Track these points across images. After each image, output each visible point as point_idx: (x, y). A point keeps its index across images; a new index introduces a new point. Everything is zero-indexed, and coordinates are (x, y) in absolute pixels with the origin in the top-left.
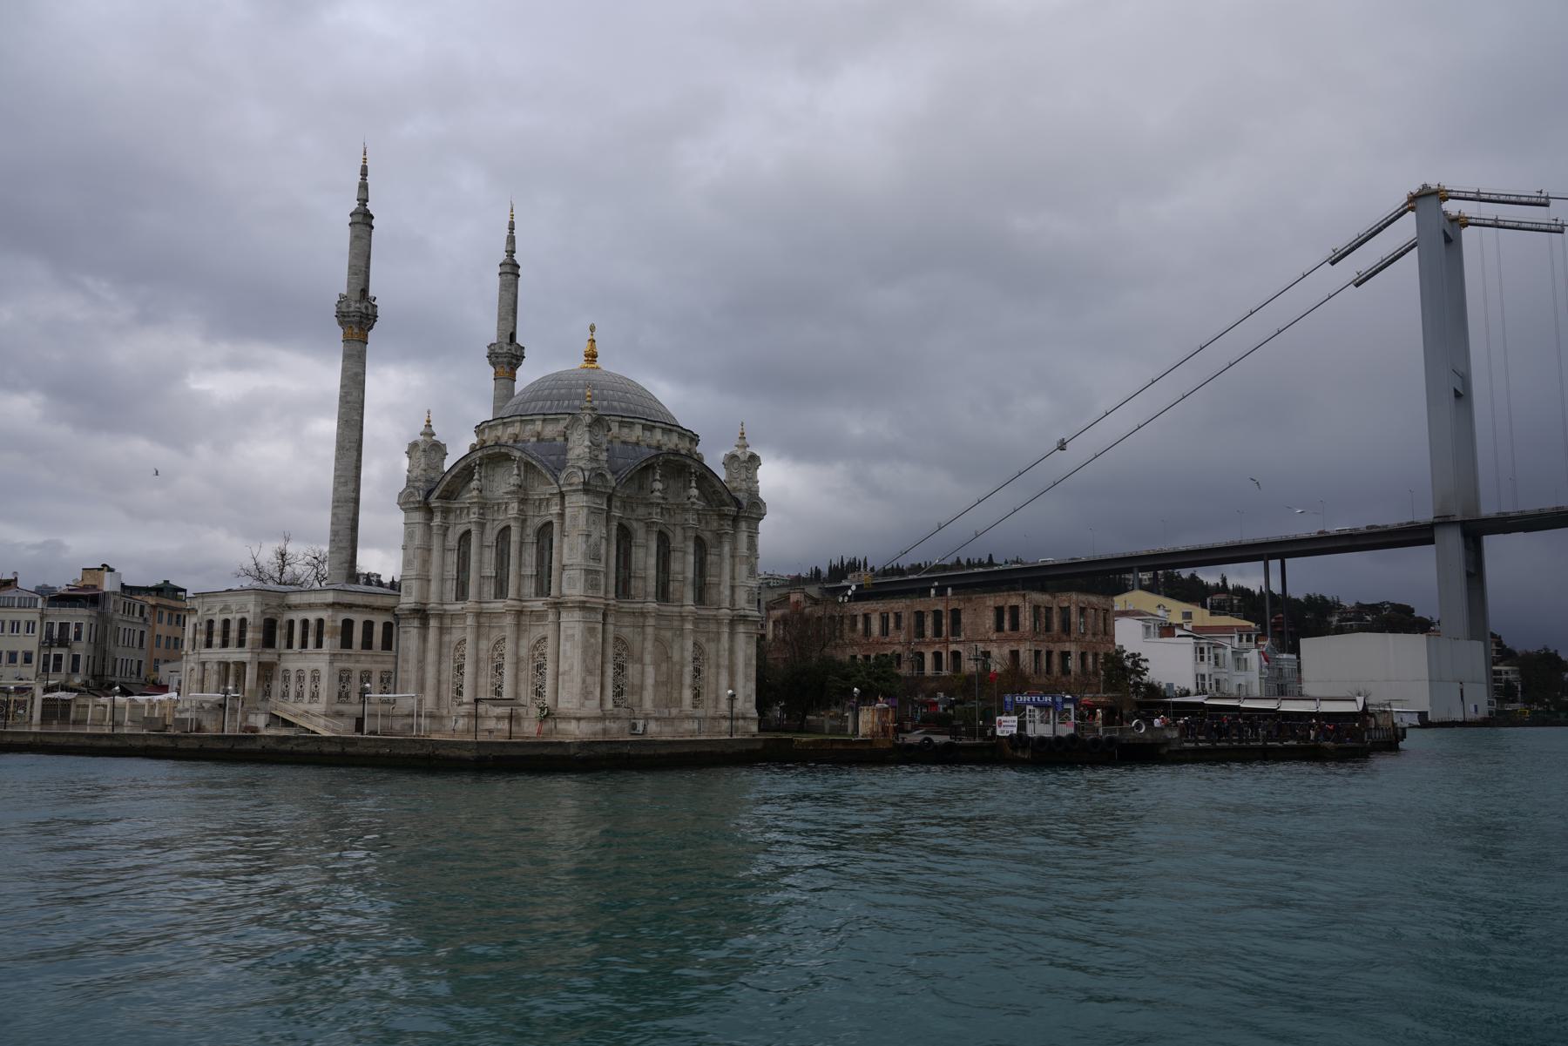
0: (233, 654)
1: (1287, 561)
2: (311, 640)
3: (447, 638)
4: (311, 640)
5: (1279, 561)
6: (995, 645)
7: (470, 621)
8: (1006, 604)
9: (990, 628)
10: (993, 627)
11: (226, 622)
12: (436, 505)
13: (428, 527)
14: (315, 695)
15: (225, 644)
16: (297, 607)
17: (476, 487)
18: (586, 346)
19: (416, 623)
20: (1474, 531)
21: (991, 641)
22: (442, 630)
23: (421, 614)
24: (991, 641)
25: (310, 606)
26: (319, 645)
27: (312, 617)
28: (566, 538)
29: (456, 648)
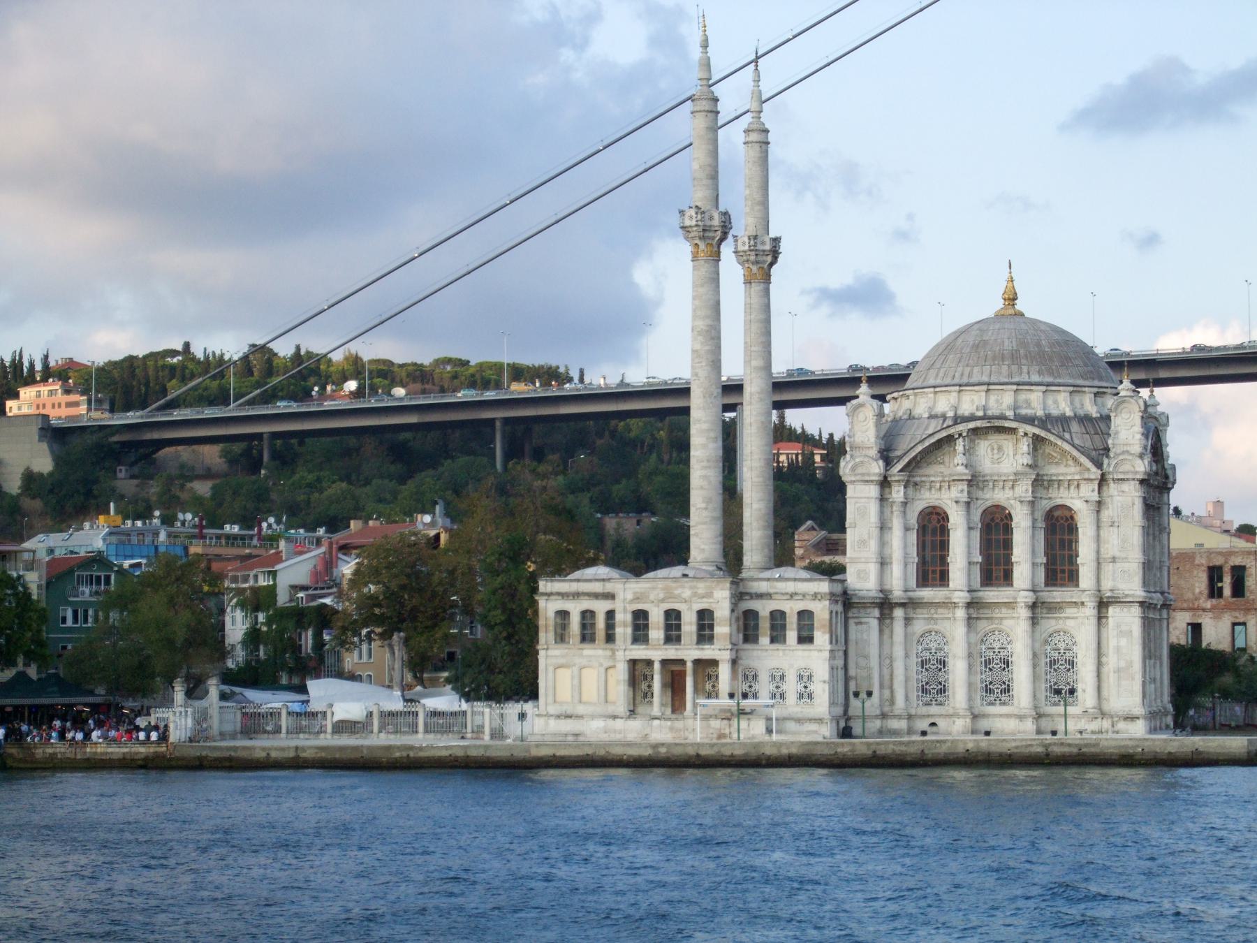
0: (689, 651)
2: (792, 635)
3: (910, 629)
4: (792, 635)
6: (1210, 615)
7: (961, 613)
8: (1226, 562)
9: (1201, 593)
10: (1206, 592)
11: (673, 619)
12: (897, 478)
13: (882, 499)
14: (805, 695)
16: (768, 596)
17: (960, 462)
18: (1002, 286)
19: (876, 613)
21: (1204, 610)
22: (908, 620)
23: (885, 605)
24: (1204, 610)
26: (806, 638)
27: (791, 608)
28: (1115, 529)
29: (919, 641)
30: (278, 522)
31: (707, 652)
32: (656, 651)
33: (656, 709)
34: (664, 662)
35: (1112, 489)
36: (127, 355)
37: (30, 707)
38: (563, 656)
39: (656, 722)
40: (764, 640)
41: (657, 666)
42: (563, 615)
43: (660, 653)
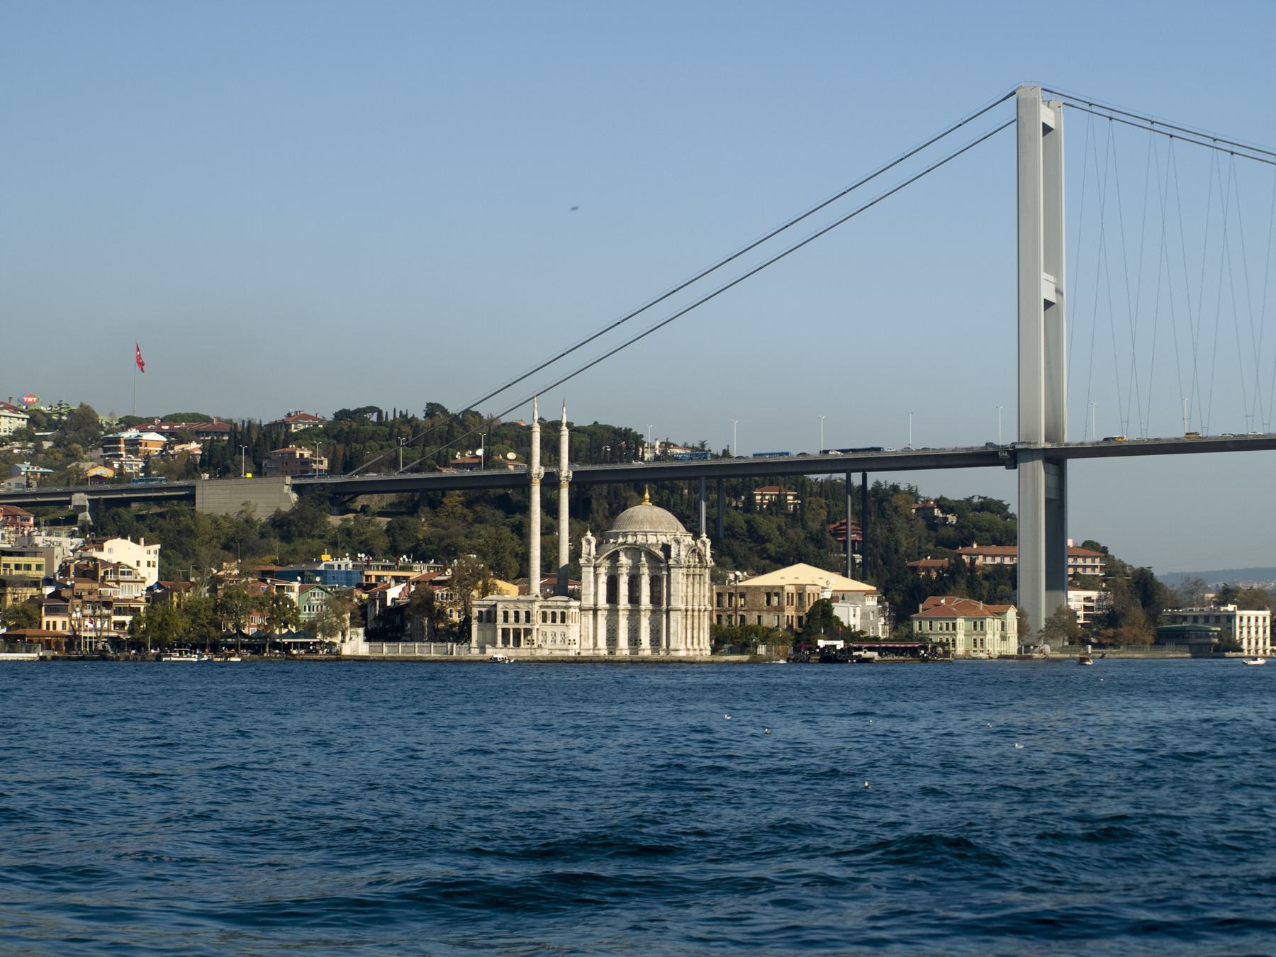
0: (522, 625)
1: (869, 474)
2: (558, 620)
4: (558, 620)
5: (860, 474)
11: (517, 614)
15: (517, 620)
19: (591, 612)
20: (1056, 459)
25: (558, 607)
26: (563, 621)
30: (408, 557)
31: (528, 626)
32: (511, 625)
33: (511, 646)
34: (514, 629)
35: (672, 570)
36: (341, 409)
37: (295, 643)
40: (549, 622)
41: (511, 631)
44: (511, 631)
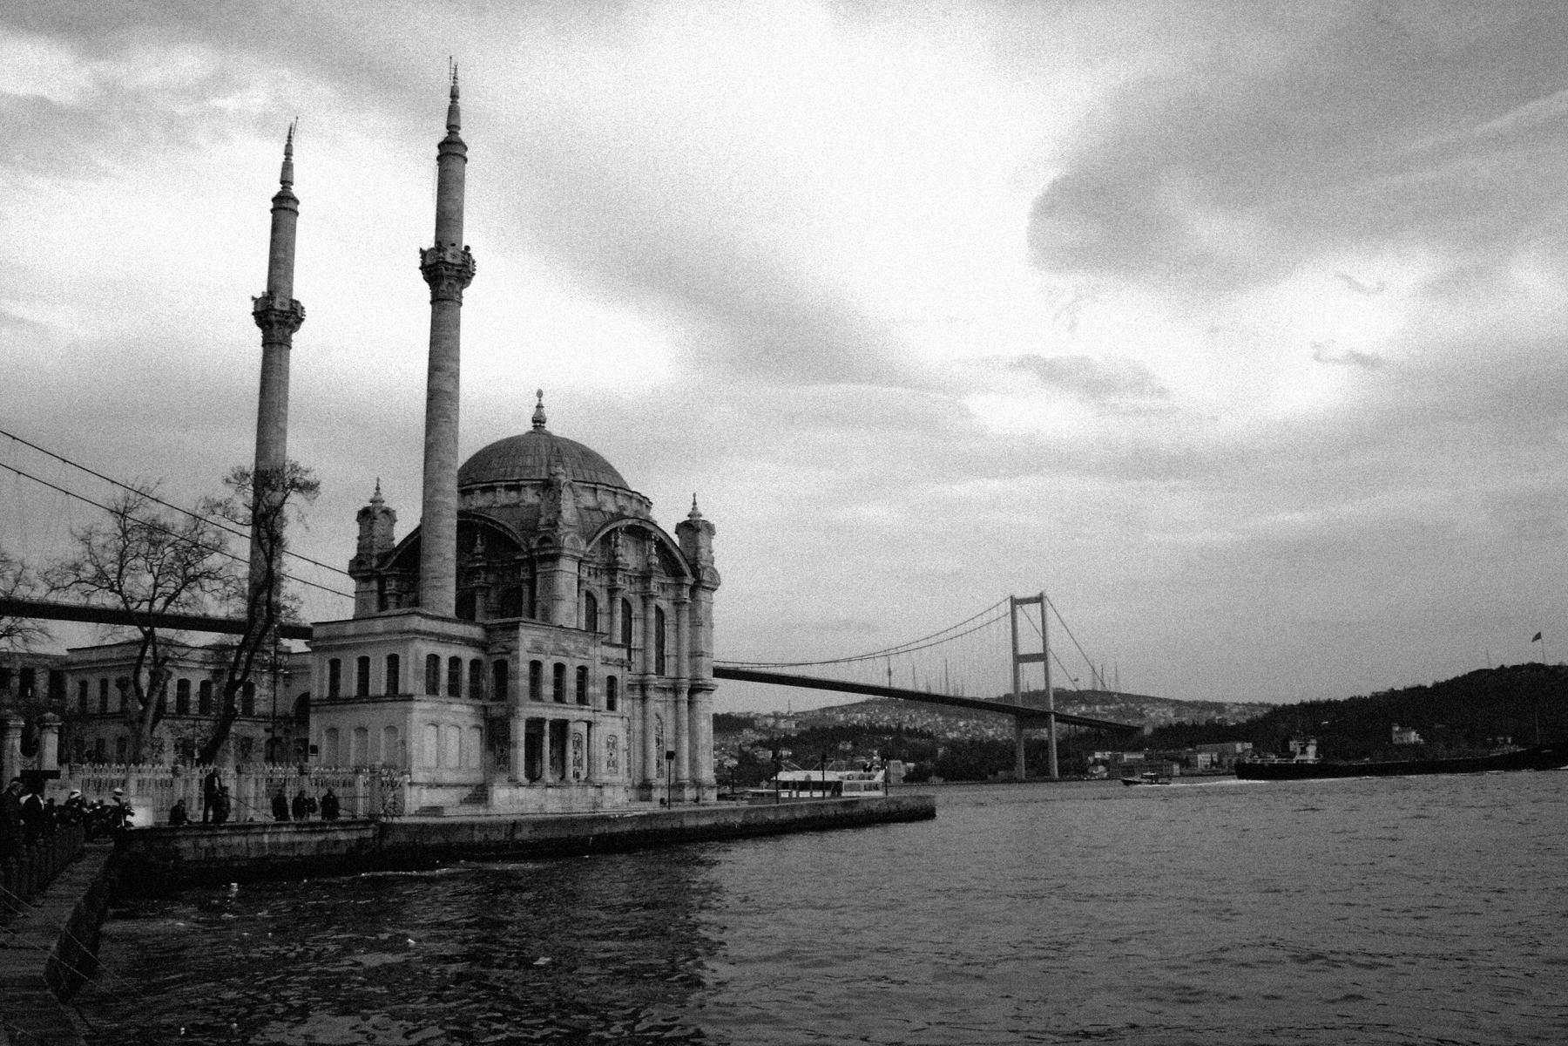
38: (433, 710)
39: (550, 791)
41: (547, 727)
42: (433, 660)
43: (551, 711)
44: (547, 727)
